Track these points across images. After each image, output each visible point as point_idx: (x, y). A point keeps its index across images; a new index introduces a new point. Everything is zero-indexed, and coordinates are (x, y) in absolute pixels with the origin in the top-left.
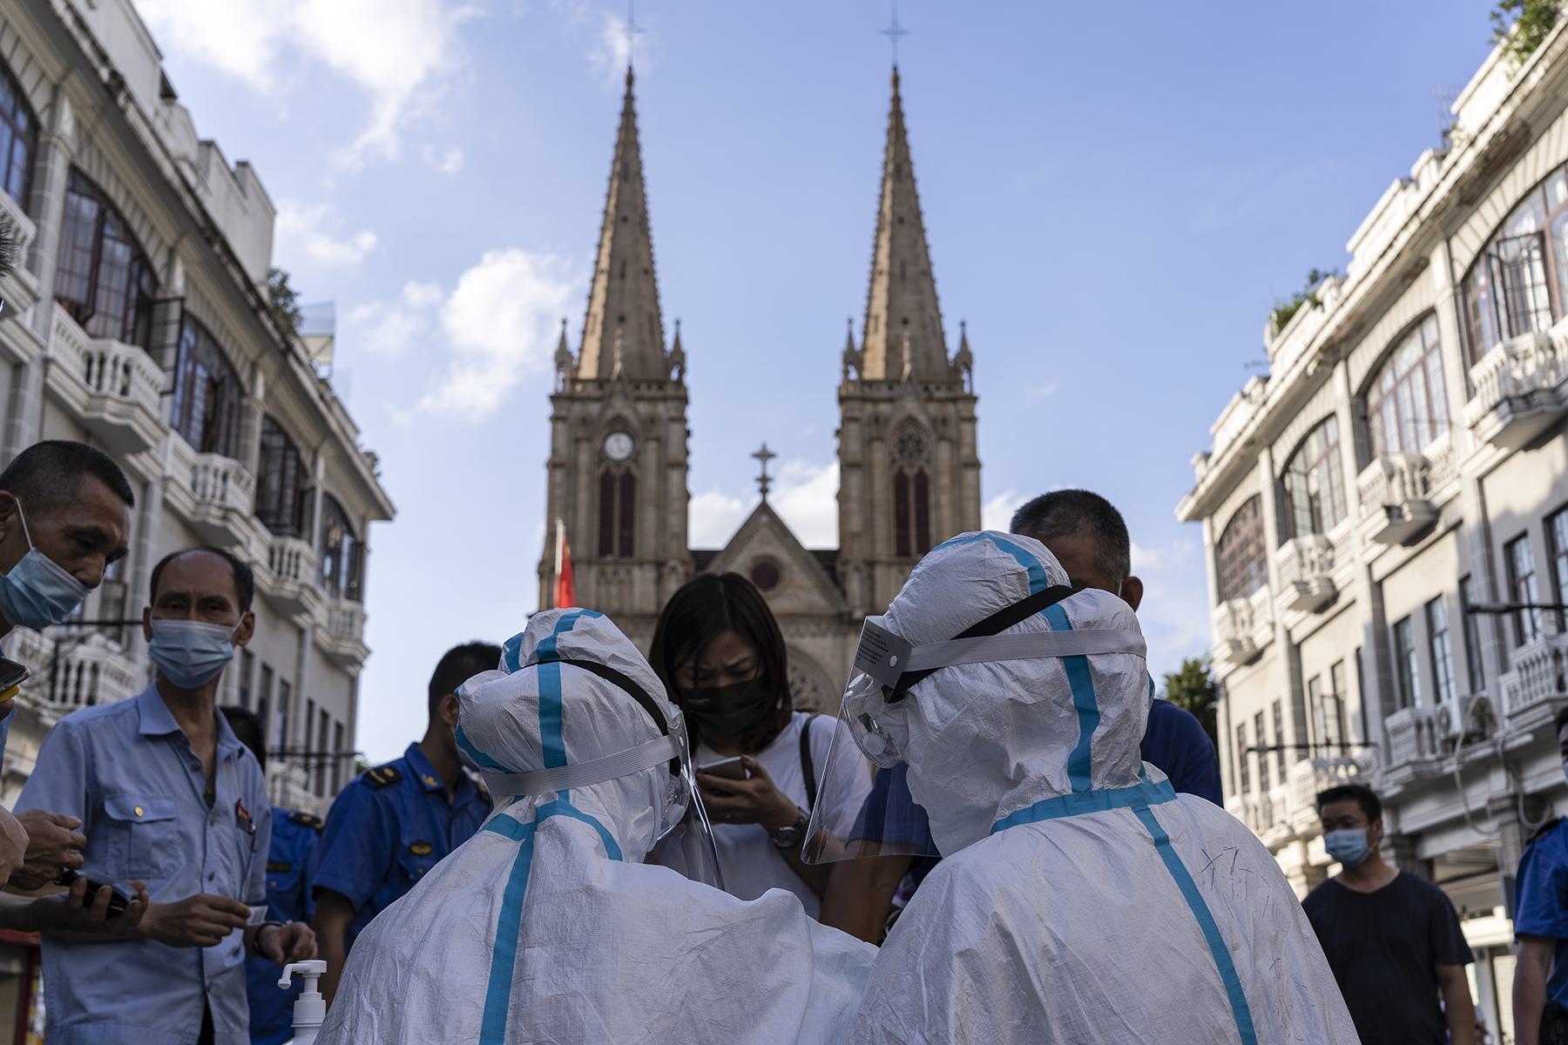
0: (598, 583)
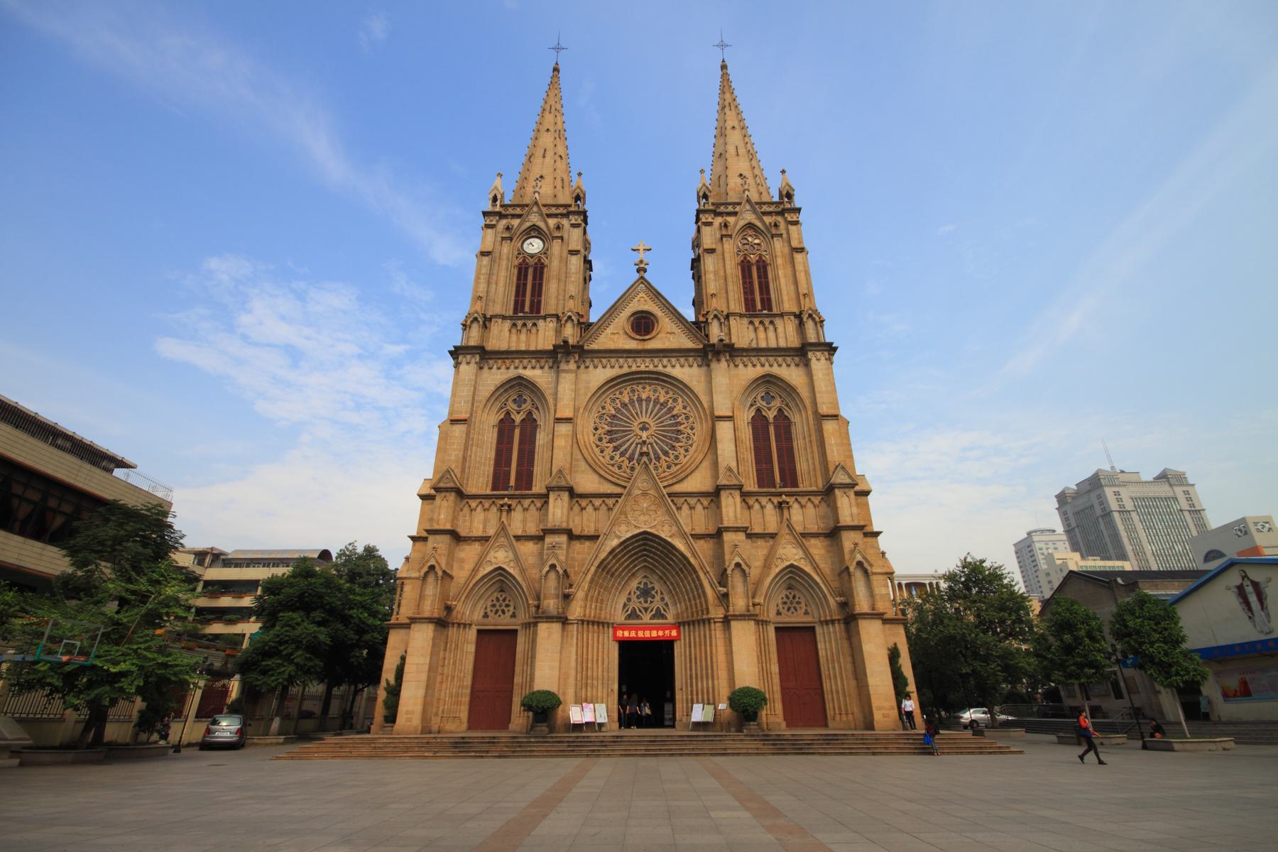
0: (510, 331)
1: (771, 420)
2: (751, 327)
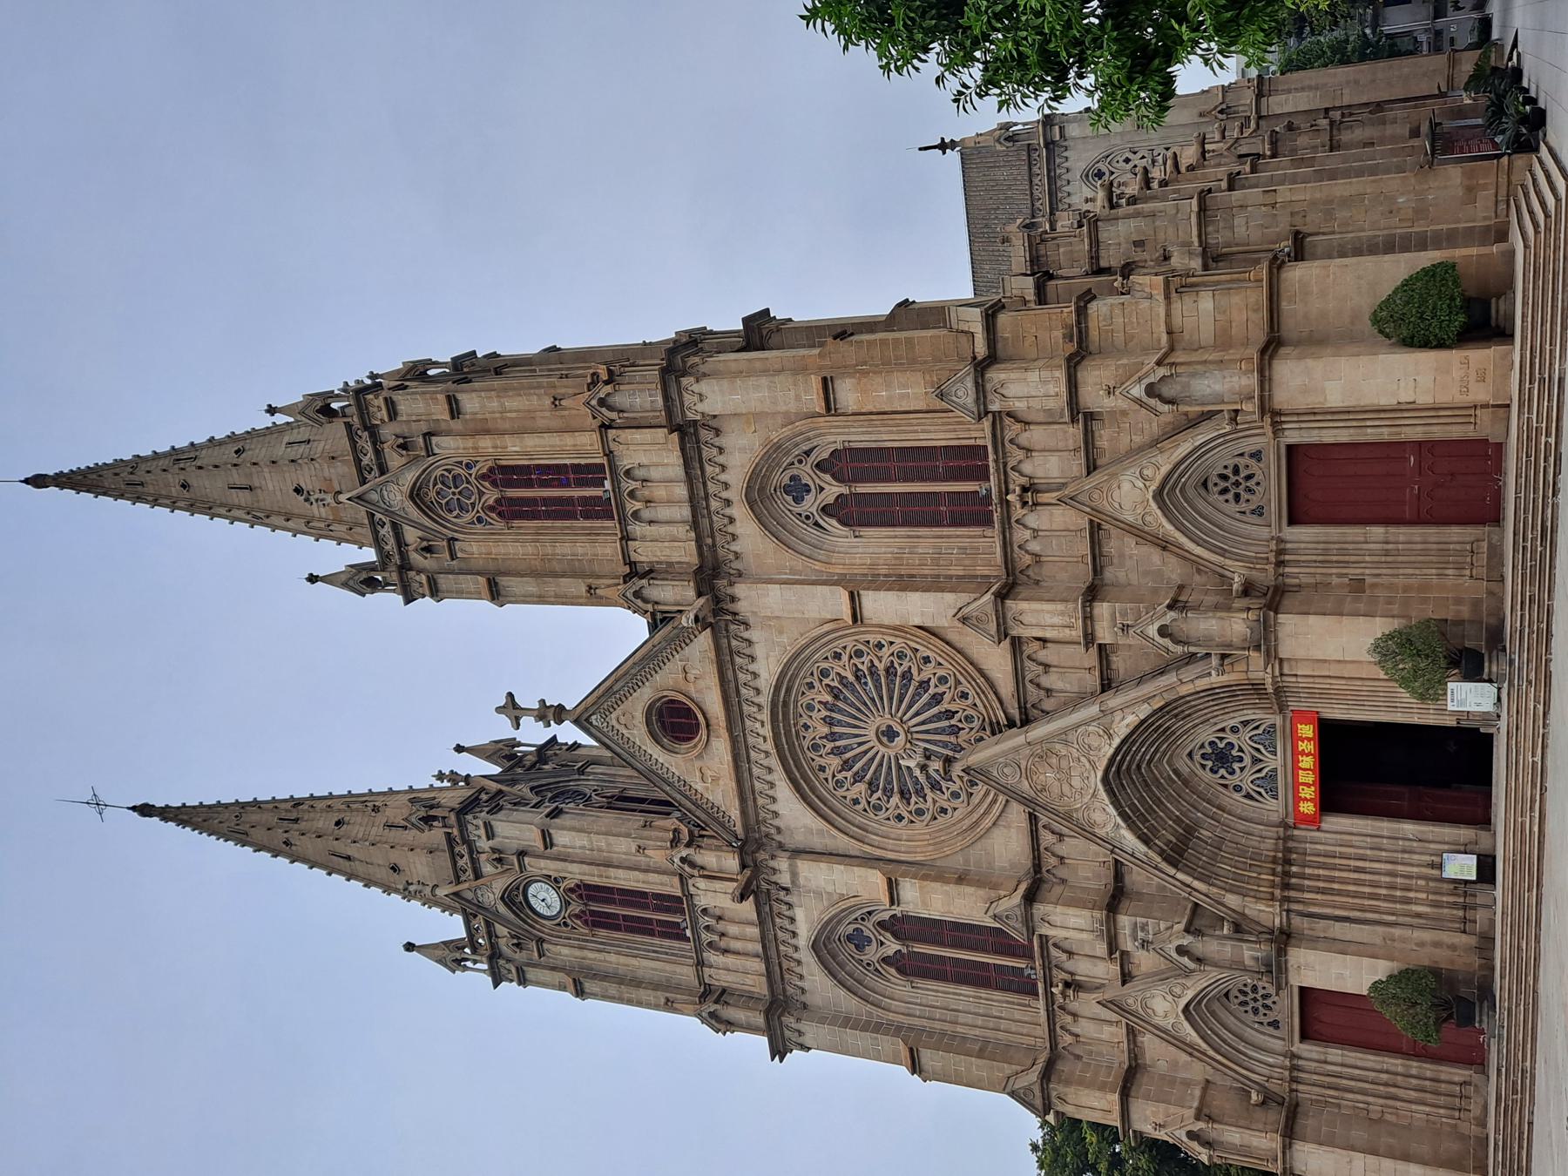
0: (726, 951)
1: (845, 490)
2: (646, 514)
